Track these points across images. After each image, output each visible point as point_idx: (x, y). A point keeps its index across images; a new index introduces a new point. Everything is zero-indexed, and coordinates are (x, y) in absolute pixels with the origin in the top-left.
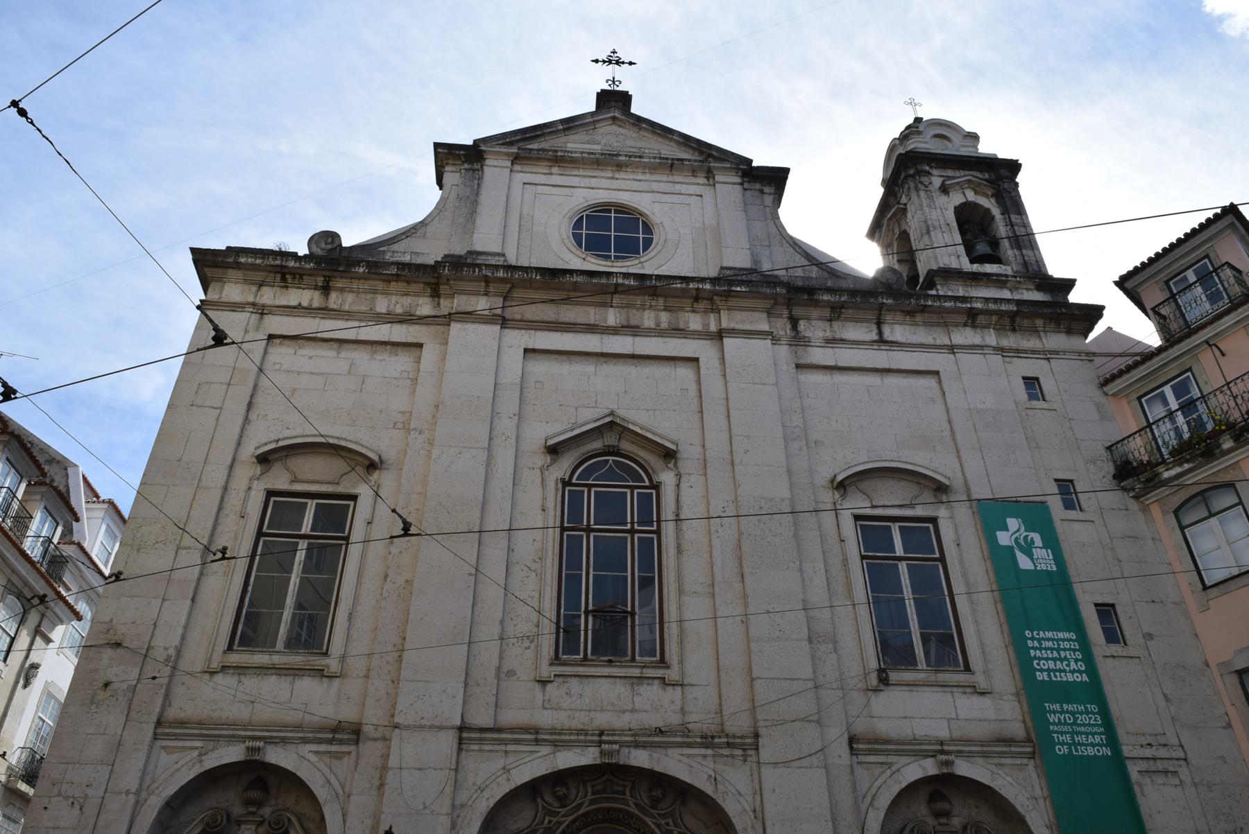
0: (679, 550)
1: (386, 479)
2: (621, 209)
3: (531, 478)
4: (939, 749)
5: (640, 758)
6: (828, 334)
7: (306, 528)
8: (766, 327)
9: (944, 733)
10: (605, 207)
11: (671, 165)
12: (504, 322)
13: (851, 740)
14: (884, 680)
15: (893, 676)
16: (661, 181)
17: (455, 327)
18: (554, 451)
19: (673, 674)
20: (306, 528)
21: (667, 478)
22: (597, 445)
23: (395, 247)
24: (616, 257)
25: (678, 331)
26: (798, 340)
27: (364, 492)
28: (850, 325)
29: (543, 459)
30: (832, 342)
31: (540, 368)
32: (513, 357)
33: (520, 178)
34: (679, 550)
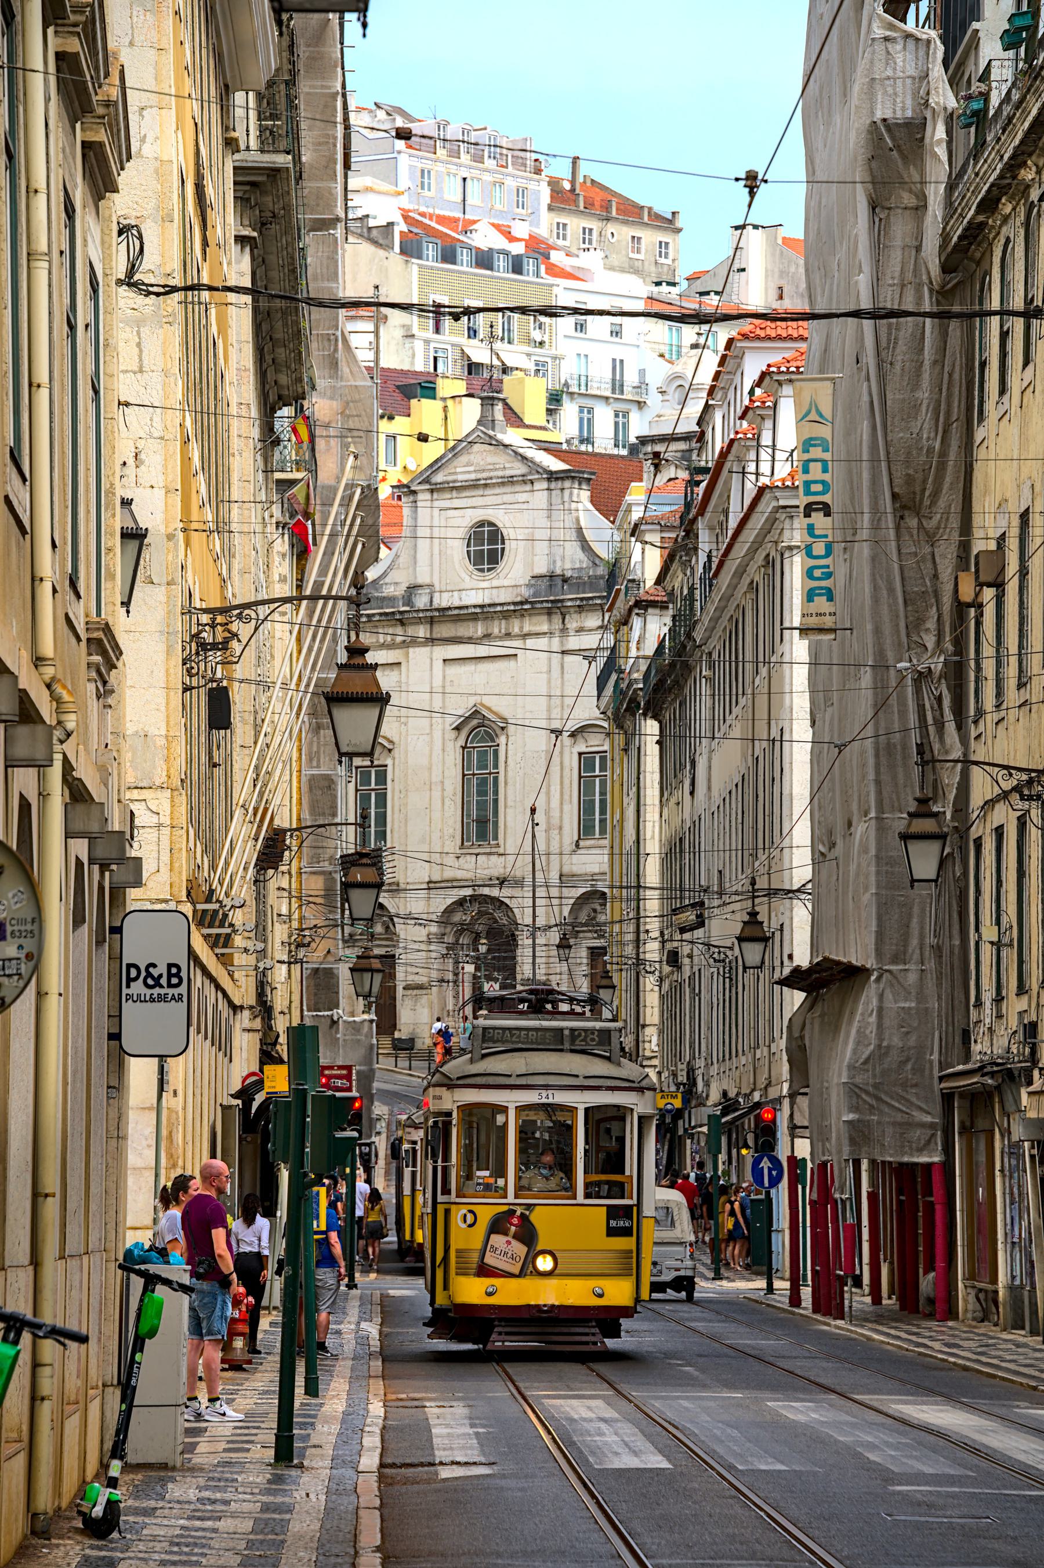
0: (506, 783)
1: (396, 753)
2: (491, 524)
3: (450, 745)
4: (593, 877)
5: (486, 891)
6: (579, 624)
7: (373, 786)
8: (545, 628)
9: (597, 871)
10: (481, 524)
11: (510, 481)
12: (431, 641)
13: (561, 875)
14: (577, 846)
15: (582, 843)
16: (506, 495)
17: (411, 650)
18: (457, 728)
19: (501, 850)
20: (373, 786)
21: (502, 740)
22: (475, 722)
23: (387, 580)
24: (489, 570)
25: (508, 635)
26: (564, 630)
27: (389, 762)
28: (590, 614)
29: (454, 734)
30: (580, 630)
31: (453, 670)
32: (438, 664)
33: (436, 504)
34: (506, 783)
